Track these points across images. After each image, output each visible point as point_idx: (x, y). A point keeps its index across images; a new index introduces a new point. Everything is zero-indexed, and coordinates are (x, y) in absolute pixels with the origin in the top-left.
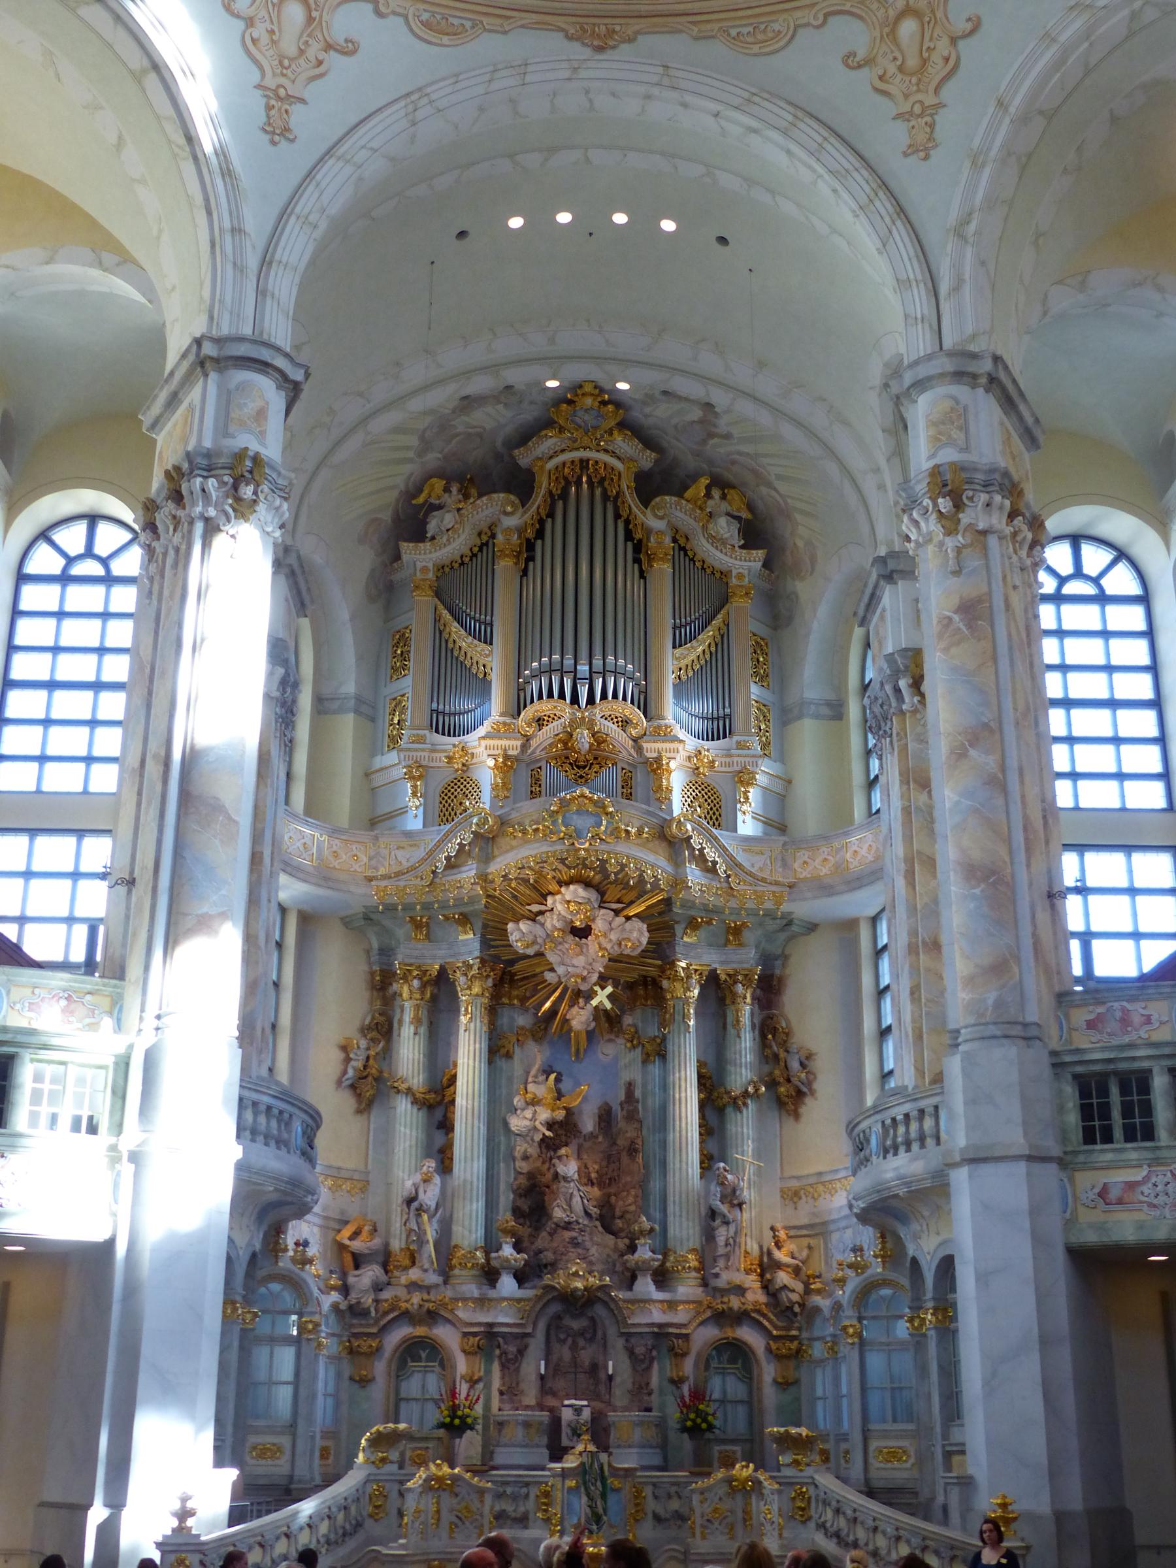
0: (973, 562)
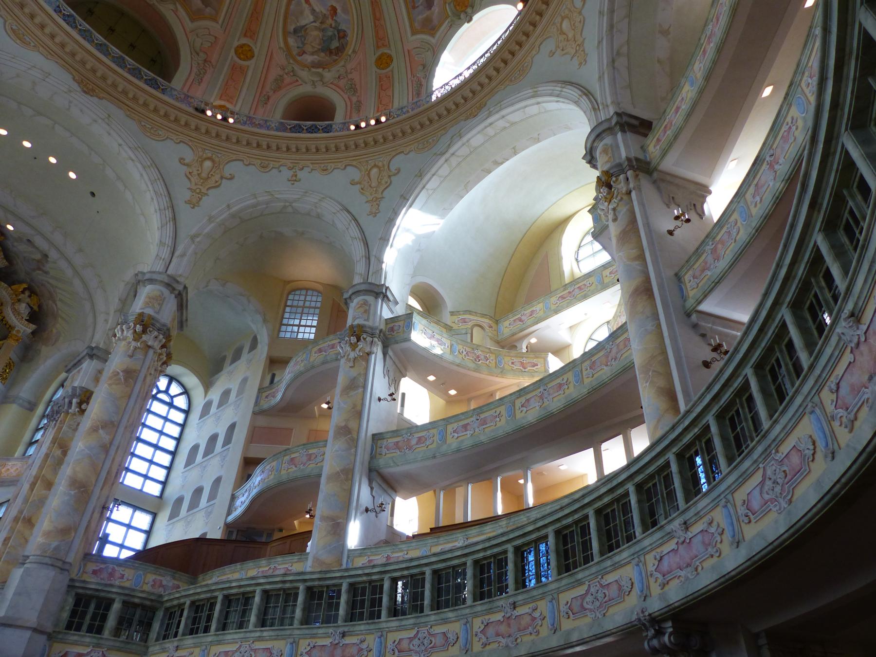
0: (139, 355)
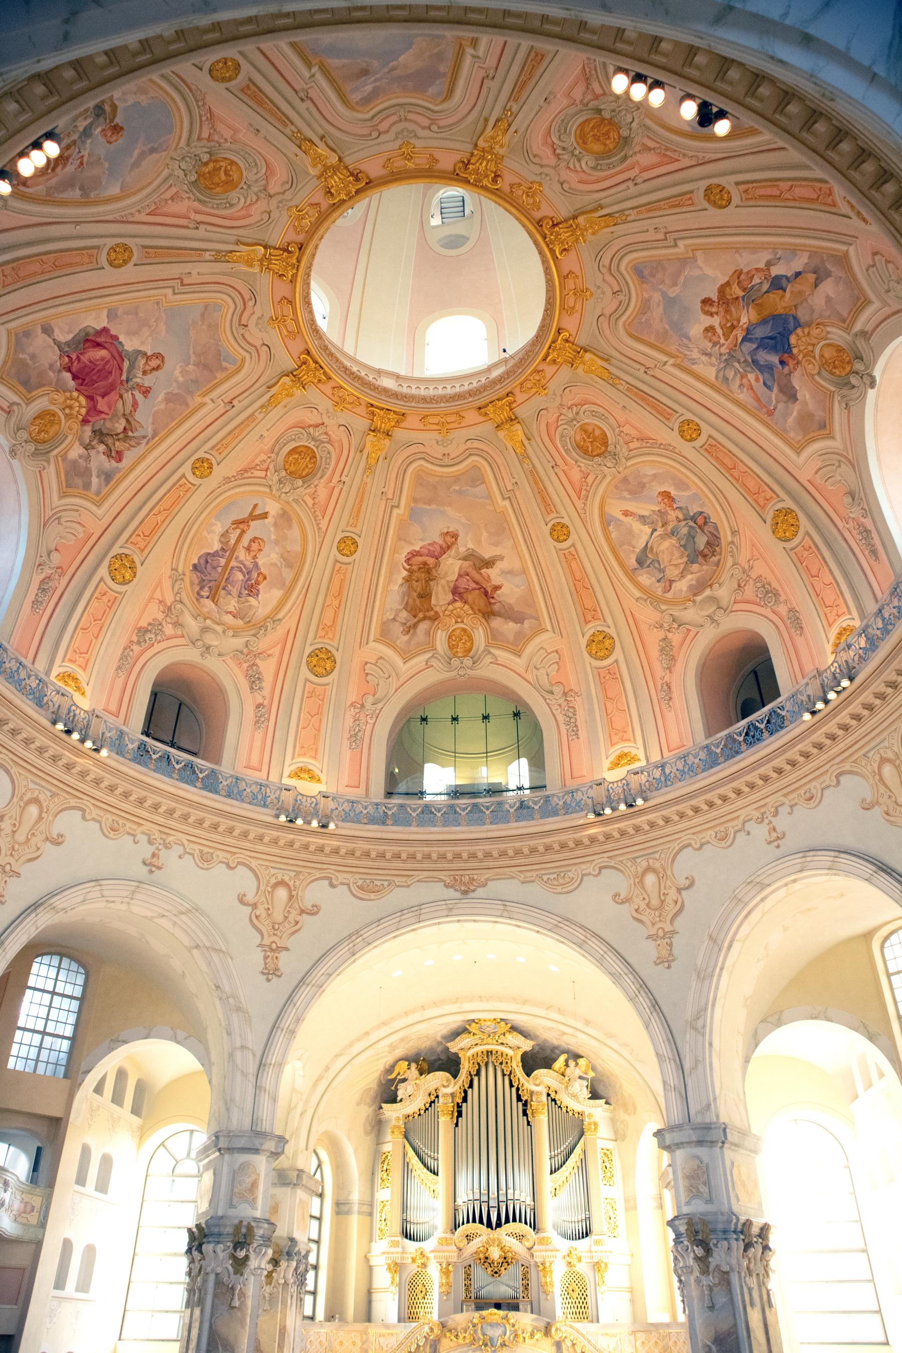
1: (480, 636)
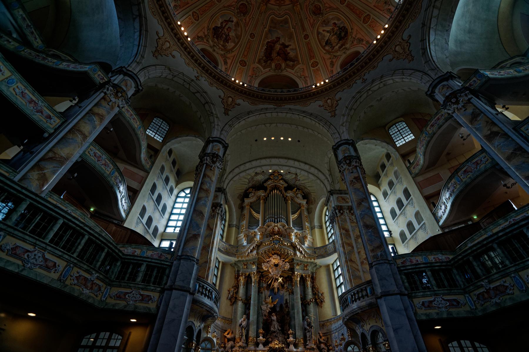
0: (355, 171)
1: (283, 65)
